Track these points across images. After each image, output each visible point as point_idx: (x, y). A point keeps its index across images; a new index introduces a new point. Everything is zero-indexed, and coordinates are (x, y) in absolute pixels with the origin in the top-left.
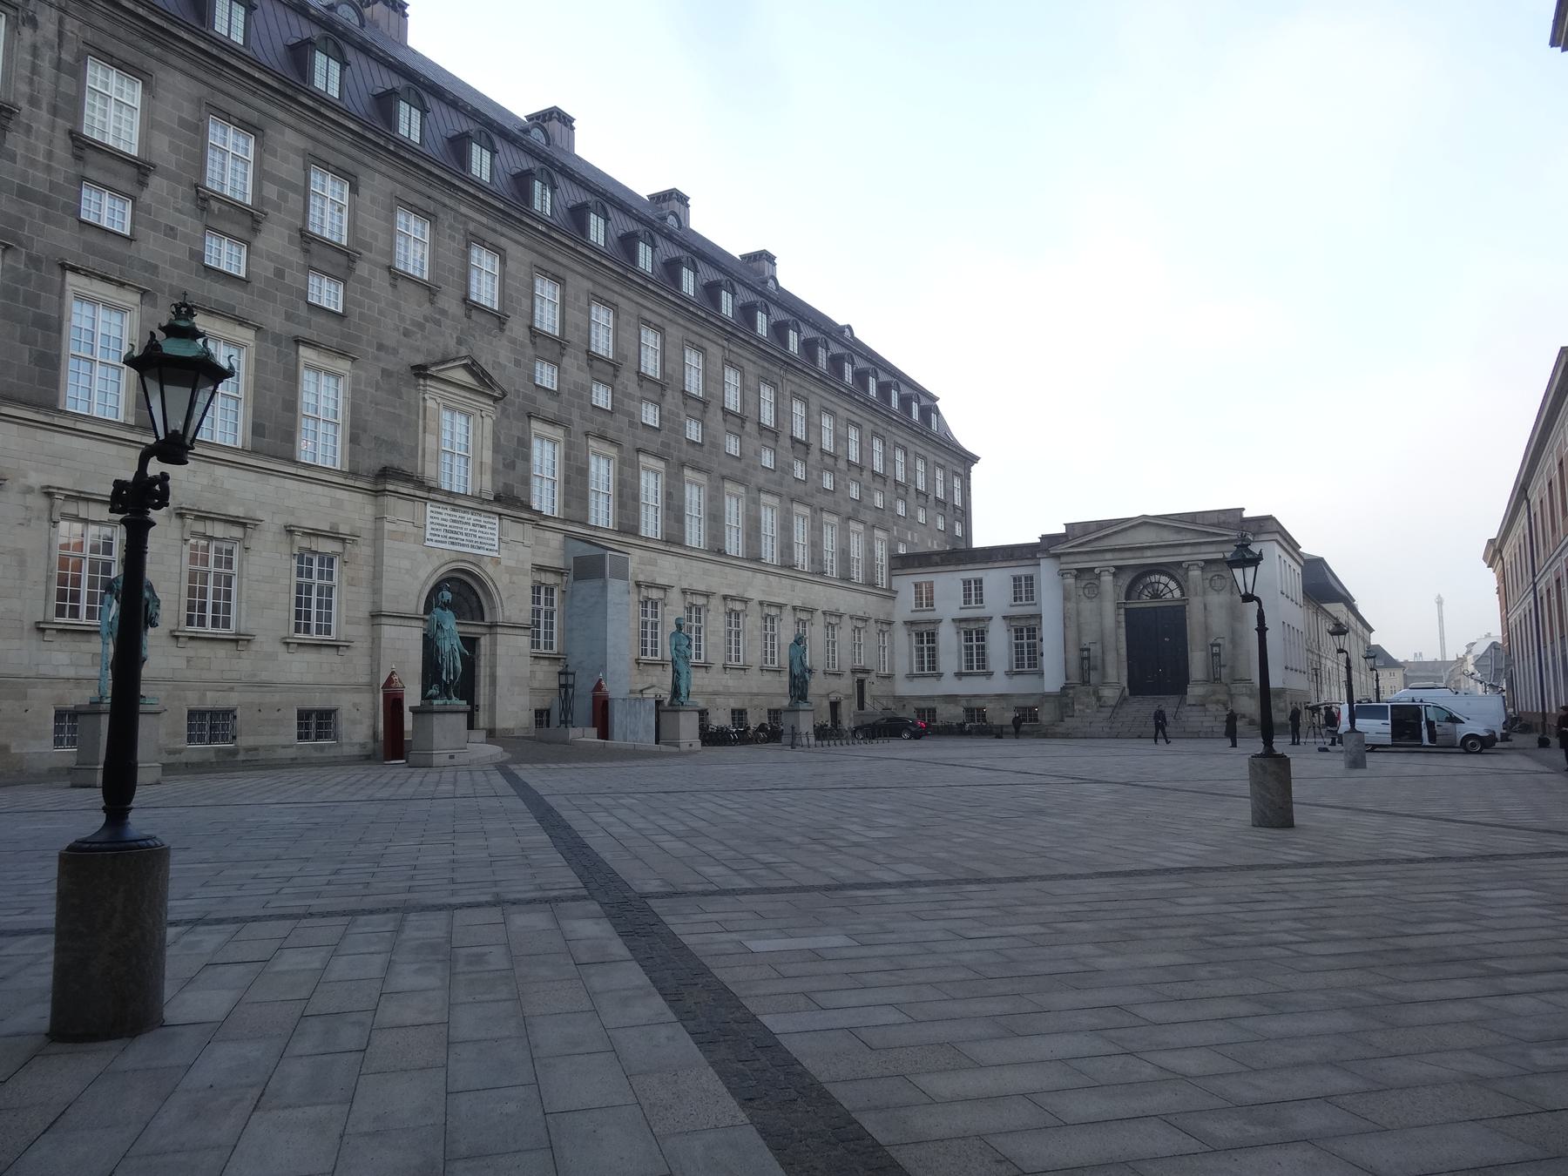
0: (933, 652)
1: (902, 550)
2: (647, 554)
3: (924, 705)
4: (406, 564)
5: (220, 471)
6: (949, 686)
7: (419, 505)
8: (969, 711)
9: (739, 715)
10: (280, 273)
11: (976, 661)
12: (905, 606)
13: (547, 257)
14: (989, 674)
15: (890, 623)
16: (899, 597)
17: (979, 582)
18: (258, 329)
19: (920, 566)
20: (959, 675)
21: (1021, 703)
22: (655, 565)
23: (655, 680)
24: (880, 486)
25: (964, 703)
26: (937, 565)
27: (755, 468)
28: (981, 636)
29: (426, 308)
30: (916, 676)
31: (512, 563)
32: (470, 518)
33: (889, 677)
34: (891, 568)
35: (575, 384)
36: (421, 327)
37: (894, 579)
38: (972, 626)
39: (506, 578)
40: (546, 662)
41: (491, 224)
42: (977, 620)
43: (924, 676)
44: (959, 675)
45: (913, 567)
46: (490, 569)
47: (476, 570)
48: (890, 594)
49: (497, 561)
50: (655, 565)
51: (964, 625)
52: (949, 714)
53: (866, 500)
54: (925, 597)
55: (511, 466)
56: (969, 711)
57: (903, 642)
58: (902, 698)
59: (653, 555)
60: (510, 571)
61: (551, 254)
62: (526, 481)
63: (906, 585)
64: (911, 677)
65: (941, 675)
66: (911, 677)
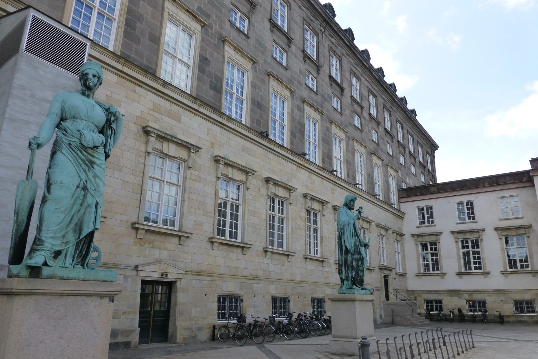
0: (435, 257)
1: (404, 186)
3: (432, 297)
6: (452, 282)
8: (472, 304)
11: (474, 262)
12: (411, 222)
14: (486, 274)
15: (402, 235)
16: (406, 217)
17: (470, 204)
19: (421, 195)
20: (460, 274)
21: (519, 297)
22: (178, 119)
23: (164, 254)
24: (390, 141)
25: (466, 296)
26: (435, 193)
27: (300, 83)
28: (476, 243)
30: (424, 275)
33: (403, 275)
34: (400, 198)
37: (401, 204)
38: (468, 236)
42: (472, 232)
43: (430, 275)
44: (460, 274)
45: (416, 195)
48: (400, 215)
50: (178, 119)
51: (461, 236)
52: (450, 304)
53: (382, 146)
54: (427, 216)
56: (472, 304)
57: (412, 248)
58: (413, 292)
59: (176, 109)
63: (411, 209)
64: (419, 275)
65: (444, 274)
66: (419, 275)
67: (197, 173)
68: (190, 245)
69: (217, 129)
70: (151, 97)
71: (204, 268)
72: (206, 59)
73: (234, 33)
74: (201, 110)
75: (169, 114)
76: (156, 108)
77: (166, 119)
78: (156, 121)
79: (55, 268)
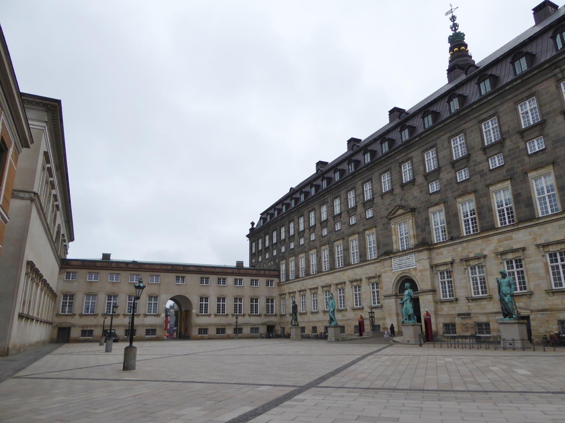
2: (503, 236)
4: (388, 280)
5: (355, 269)
7: (389, 261)
9: (314, 329)
10: (361, 217)
13: (430, 142)
18: (358, 233)
29: (392, 198)
31: (421, 268)
32: (405, 258)
35: (447, 181)
36: (390, 204)
39: (419, 274)
40: (448, 303)
41: (406, 153)
46: (413, 273)
47: (408, 275)
49: (415, 269)
50: (511, 238)
55: (423, 230)
60: (421, 271)
61: (429, 140)
62: (430, 233)
67: (529, 259)
68: (536, 297)
69: (535, 229)
70: (496, 238)
71: (547, 307)
72: (519, 194)
73: (534, 159)
74: (519, 227)
75: (506, 239)
76: (500, 241)
77: (505, 243)
78: (501, 246)
79: (405, 321)
